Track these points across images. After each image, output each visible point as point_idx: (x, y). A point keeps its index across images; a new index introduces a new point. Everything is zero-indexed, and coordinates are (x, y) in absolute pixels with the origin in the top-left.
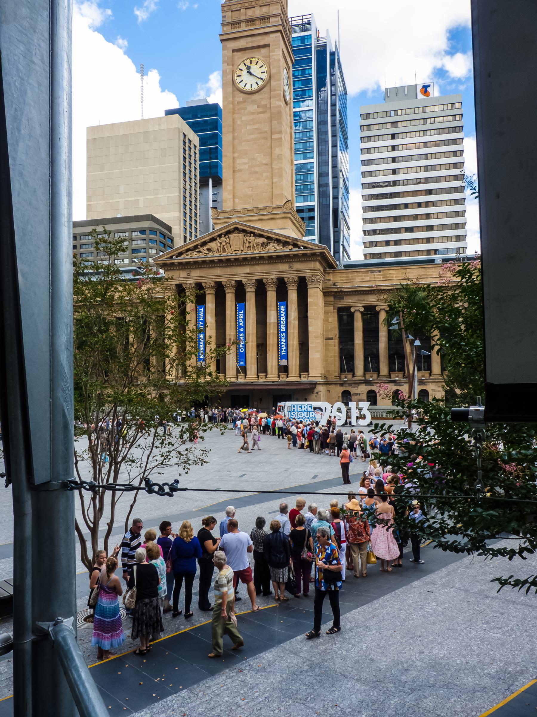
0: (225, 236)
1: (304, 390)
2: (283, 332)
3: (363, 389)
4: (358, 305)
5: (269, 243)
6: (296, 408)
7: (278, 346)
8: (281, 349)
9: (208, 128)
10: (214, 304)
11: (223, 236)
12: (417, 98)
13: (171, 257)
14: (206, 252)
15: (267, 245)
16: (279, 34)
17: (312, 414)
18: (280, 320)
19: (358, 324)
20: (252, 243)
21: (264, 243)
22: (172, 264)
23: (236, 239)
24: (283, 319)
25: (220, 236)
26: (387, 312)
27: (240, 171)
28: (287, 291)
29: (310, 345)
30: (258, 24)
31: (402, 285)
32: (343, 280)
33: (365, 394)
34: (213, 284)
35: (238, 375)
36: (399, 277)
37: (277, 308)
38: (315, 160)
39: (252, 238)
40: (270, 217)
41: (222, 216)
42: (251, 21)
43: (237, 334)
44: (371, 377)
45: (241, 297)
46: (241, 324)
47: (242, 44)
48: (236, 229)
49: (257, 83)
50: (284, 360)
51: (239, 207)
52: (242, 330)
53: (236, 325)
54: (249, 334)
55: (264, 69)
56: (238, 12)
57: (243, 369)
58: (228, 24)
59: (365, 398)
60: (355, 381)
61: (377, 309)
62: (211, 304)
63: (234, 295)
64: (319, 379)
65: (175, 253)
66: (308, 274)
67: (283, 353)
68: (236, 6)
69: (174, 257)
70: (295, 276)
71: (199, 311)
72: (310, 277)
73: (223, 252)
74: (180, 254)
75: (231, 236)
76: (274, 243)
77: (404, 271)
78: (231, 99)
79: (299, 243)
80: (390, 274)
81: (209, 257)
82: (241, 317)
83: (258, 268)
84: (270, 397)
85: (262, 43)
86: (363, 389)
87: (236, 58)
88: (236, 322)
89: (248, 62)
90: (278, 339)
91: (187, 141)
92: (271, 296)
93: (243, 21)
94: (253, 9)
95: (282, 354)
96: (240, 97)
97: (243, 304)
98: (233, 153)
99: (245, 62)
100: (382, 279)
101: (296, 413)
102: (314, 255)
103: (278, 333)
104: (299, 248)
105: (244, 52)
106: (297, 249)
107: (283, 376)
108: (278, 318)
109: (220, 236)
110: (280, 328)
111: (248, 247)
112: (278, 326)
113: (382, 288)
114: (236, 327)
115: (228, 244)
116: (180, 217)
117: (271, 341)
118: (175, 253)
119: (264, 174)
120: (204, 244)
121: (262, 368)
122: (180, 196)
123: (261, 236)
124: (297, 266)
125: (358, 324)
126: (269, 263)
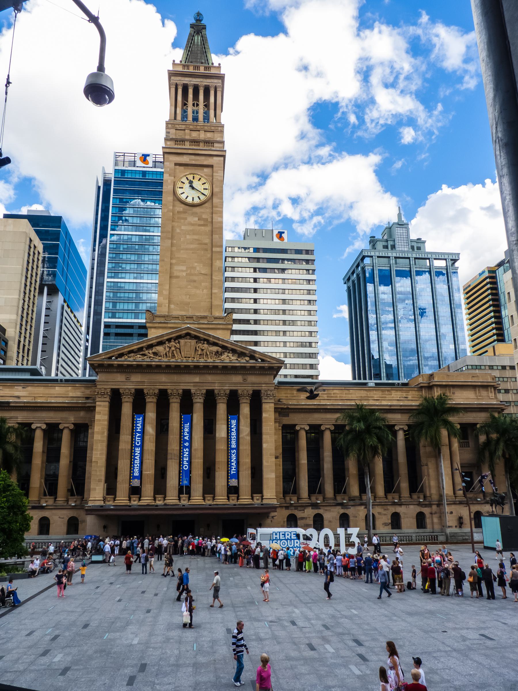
0: (175, 340)
1: (259, 514)
2: (233, 449)
3: (310, 513)
4: (303, 423)
5: (224, 352)
6: (278, 536)
7: (228, 464)
8: (230, 467)
9: (49, 238)
10: (155, 414)
11: (173, 340)
12: (273, 240)
13: (110, 358)
14: (152, 356)
15: (221, 355)
16: (222, 159)
17: (297, 543)
18: (231, 435)
19: (303, 443)
20: (205, 351)
21: (217, 352)
22: (111, 366)
24: (234, 434)
25: (169, 340)
26: (332, 432)
27: (177, 277)
28: (239, 404)
29: (265, 463)
30: (202, 146)
31: (358, 406)
32: (287, 397)
33: (312, 519)
34: (157, 391)
35: (181, 496)
36: (342, 397)
37: (228, 422)
39: (206, 346)
40: (211, 326)
41: (158, 320)
43: (180, 449)
44: (317, 499)
45: (187, 407)
46: (186, 438)
48: (188, 334)
49: (198, 197)
50: (234, 480)
51: (175, 313)
52: (187, 444)
53: (180, 438)
54: (195, 450)
55: (207, 186)
56: (183, 132)
57: (184, 490)
58: (171, 140)
59: (312, 523)
60: (302, 503)
61: (323, 428)
62: (151, 415)
63: (179, 405)
64: (275, 502)
65: (116, 353)
66: (264, 388)
67: (233, 471)
68: (180, 126)
69: (114, 358)
70: (250, 389)
71: (136, 421)
72: (266, 391)
73: (172, 358)
74: (121, 355)
75: (182, 341)
76: (229, 353)
77: (347, 392)
78: (171, 208)
79: (257, 356)
80: (334, 394)
81: (156, 361)
82: (187, 430)
83: (209, 378)
84: (236, 523)
85: (205, 163)
86: (310, 513)
87: (177, 171)
88: (181, 435)
89: (190, 177)
90: (228, 456)
91: (32, 246)
92: (222, 409)
93: (187, 140)
94: (198, 132)
95: (232, 472)
96: (180, 208)
97: (189, 416)
98: (171, 259)
99: (188, 176)
100: (326, 398)
101: (279, 541)
102: (271, 368)
103: (228, 450)
104: (257, 360)
105: (187, 167)
106: (254, 361)
107: (233, 498)
108: (228, 433)
109: (169, 340)
110: (231, 444)
111: (201, 355)
112: (228, 441)
113: (329, 407)
114: (180, 441)
115: (178, 350)
116: (17, 320)
117: (221, 457)
118: (116, 353)
119: (203, 284)
121: (209, 488)
122: (19, 299)
123: (215, 344)
124: (252, 379)
125: (303, 443)
126: (222, 373)
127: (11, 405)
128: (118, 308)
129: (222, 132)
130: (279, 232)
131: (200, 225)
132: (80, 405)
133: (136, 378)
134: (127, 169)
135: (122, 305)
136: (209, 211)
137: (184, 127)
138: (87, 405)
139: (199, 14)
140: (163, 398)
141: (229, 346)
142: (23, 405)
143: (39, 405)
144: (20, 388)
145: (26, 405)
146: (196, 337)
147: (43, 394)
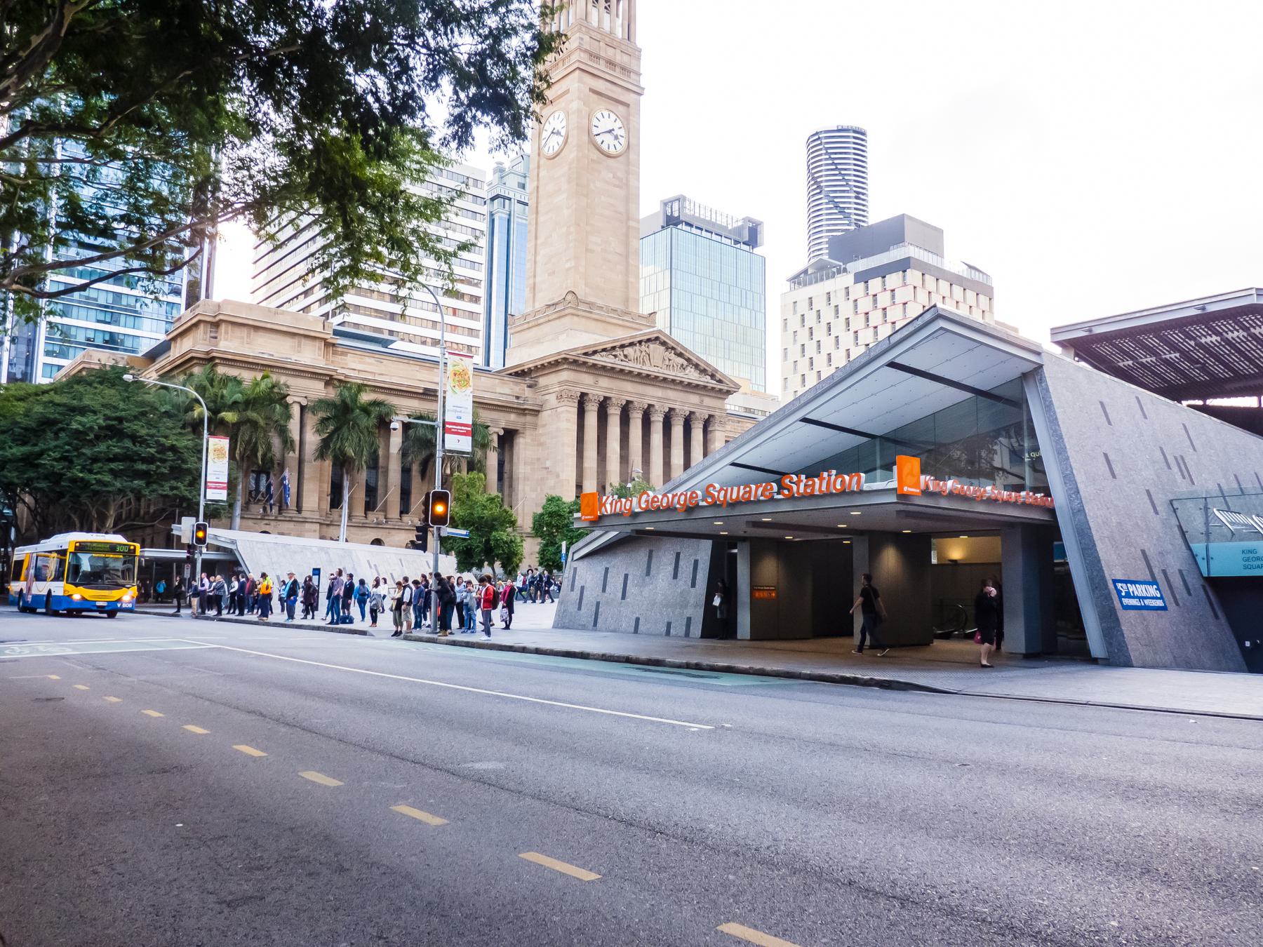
23: (656, 349)
25: (640, 342)
27: (592, 251)
39: (672, 356)
42: (611, 63)
47: (600, 85)
48: (657, 338)
58: (586, 51)
66: (717, 414)
74: (595, 352)
75: (652, 346)
81: (628, 366)
85: (621, 99)
93: (604, 59)
96: (595, 155)
120: (623, 346)
123: (680, 355)
124: (708, 401)
129: (639, 58)
137: (598, 37)
146: (664, 344)
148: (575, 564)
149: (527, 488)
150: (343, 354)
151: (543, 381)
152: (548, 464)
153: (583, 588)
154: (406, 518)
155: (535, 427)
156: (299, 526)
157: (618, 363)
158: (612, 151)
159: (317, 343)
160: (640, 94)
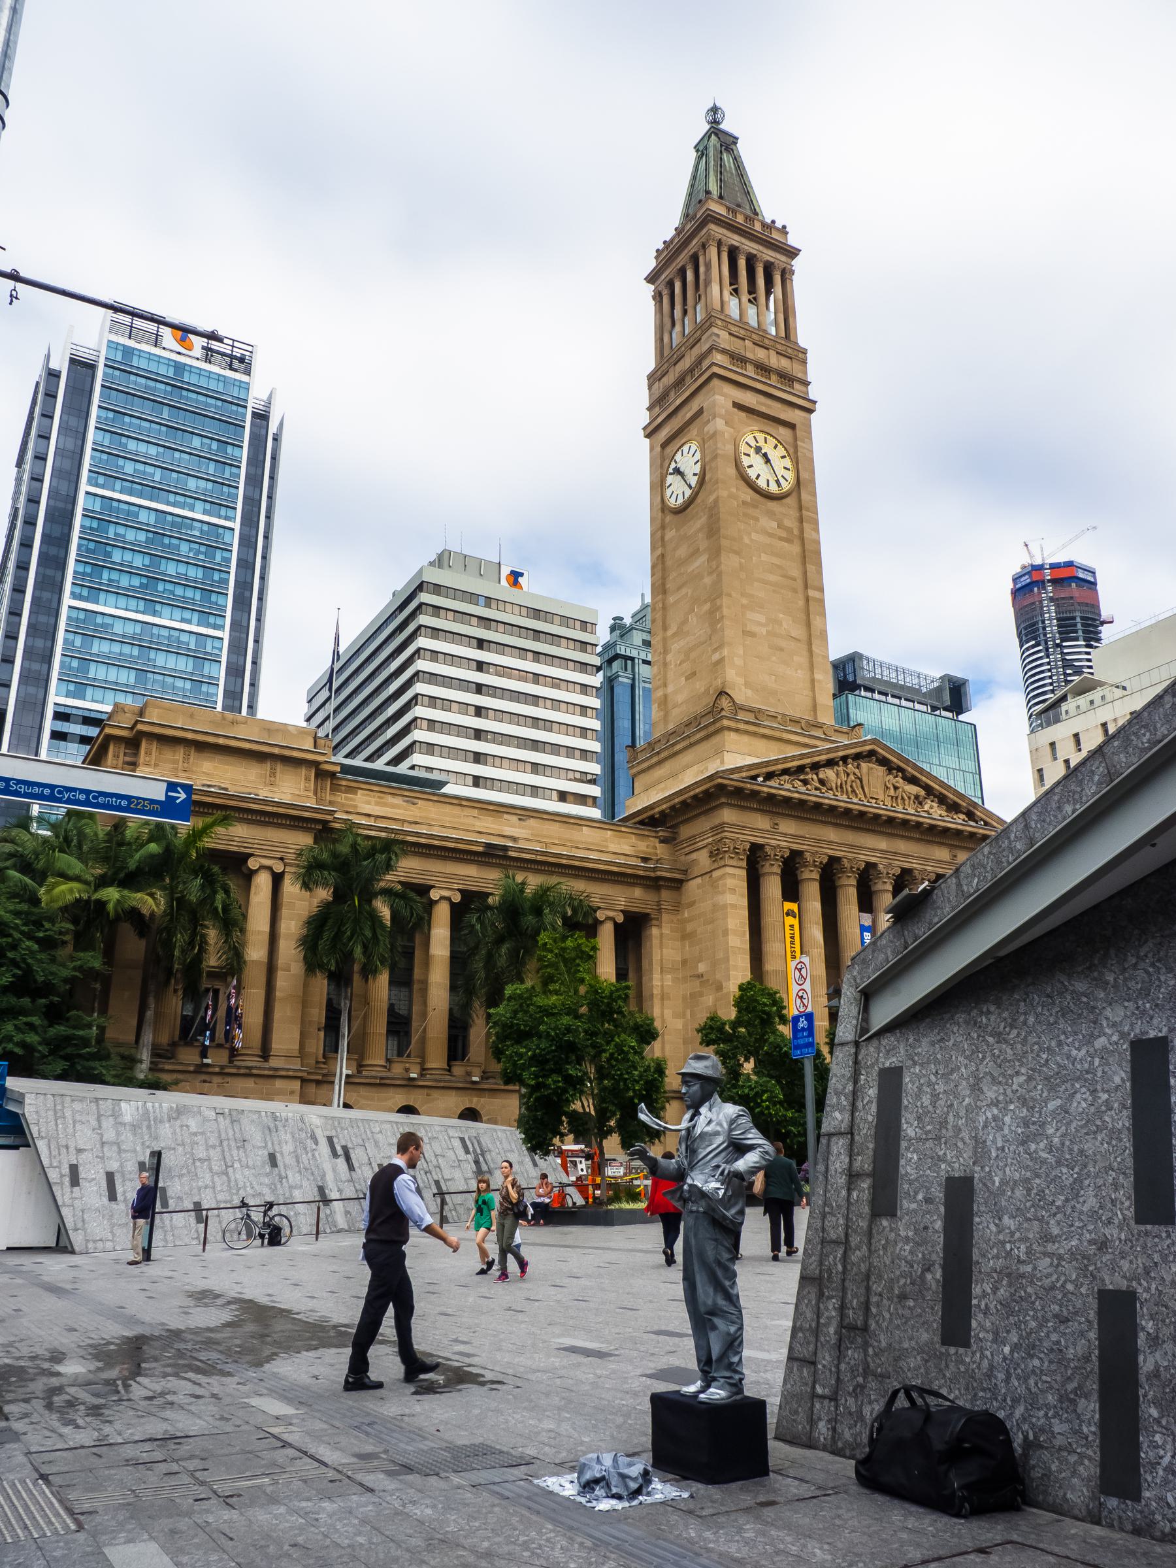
13: (754, 778)
14: (818, 785)
21: (917, 797)
23: (874, 775)
25: (844, 759)
27: (752, 635)
38: (225, 634)
39: (900, 782)
42: (763, 368)
47: (749, 399)
48: (872, 753)
58: (724, 351)
74: (769, 776)
75: (864, 765)
81: (828, 798)
85: (783, 416)
93: (751, 362)
120: (816, 767)
123: (913, 780)
127: (511, 854)
128: (92, 675)
129: (804, 362)
130: (513, 572)
131: (781, 539)
132: (641, 873)
133: (788, 827)
134: (137, 346)
135: (102, 668)
136: (794, 513)
138: (659, 873)
139: (714, 109)
140: (830, 874)
141: (937, 787)
142: (533, 857)
143: (564, 861)
144: (514, 819)
145: (539, 858)
146: (883, 762)
147: (559, 839)
148: (880, 1057)
149: (668, 1013)
150: (351, 790)
151: (685, 831)
152: (702, 968)
153: (960, 1195)
154: (458, 1070)
155: (677, 908)
156: (264, 1085)
157: (812, 794)
158: (773, 488)
159: (303, 771)
160: (811, 411)
